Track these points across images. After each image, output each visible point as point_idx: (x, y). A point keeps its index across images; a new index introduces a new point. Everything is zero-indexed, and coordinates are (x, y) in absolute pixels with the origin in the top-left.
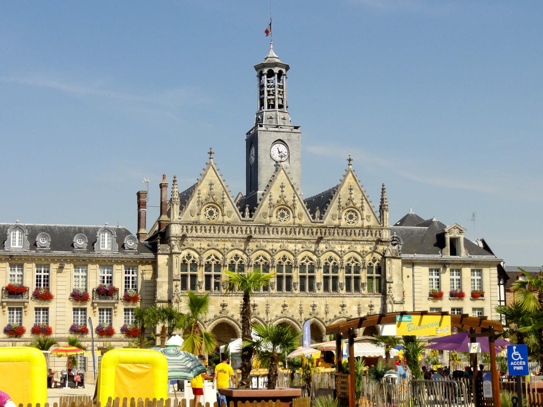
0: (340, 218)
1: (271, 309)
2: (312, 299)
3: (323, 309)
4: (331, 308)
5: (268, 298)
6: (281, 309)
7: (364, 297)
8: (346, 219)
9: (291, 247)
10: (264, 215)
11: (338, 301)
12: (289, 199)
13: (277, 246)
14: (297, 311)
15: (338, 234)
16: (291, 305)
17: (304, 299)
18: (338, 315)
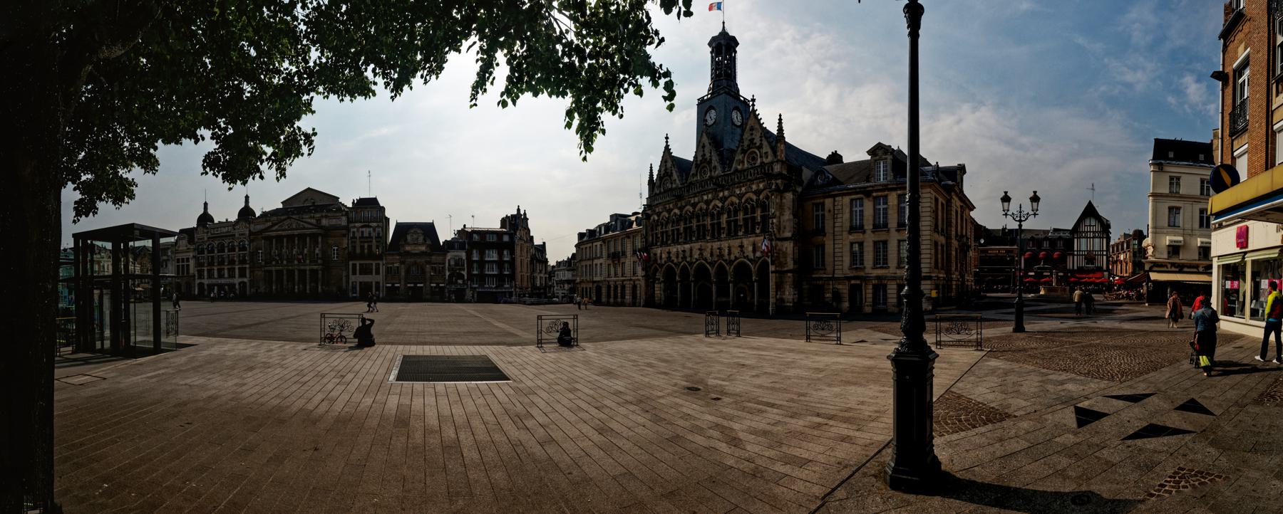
0: (743, 162)
1: (693, 253)
2: (719, 243)
3: (727, 251)
4: (733, 250)
5: (692, 245)
6: (698, 252)
7: (757, 236)
8: (749, 162)
9: (705, 197)
10: (693, 174)
11: (736, 243)
12: (708, 155)
13: (696, 199)
14: (709, 255)
15: (738, 178)
16: (705, 250)
17: (714, 244)
18: (738, 255)
